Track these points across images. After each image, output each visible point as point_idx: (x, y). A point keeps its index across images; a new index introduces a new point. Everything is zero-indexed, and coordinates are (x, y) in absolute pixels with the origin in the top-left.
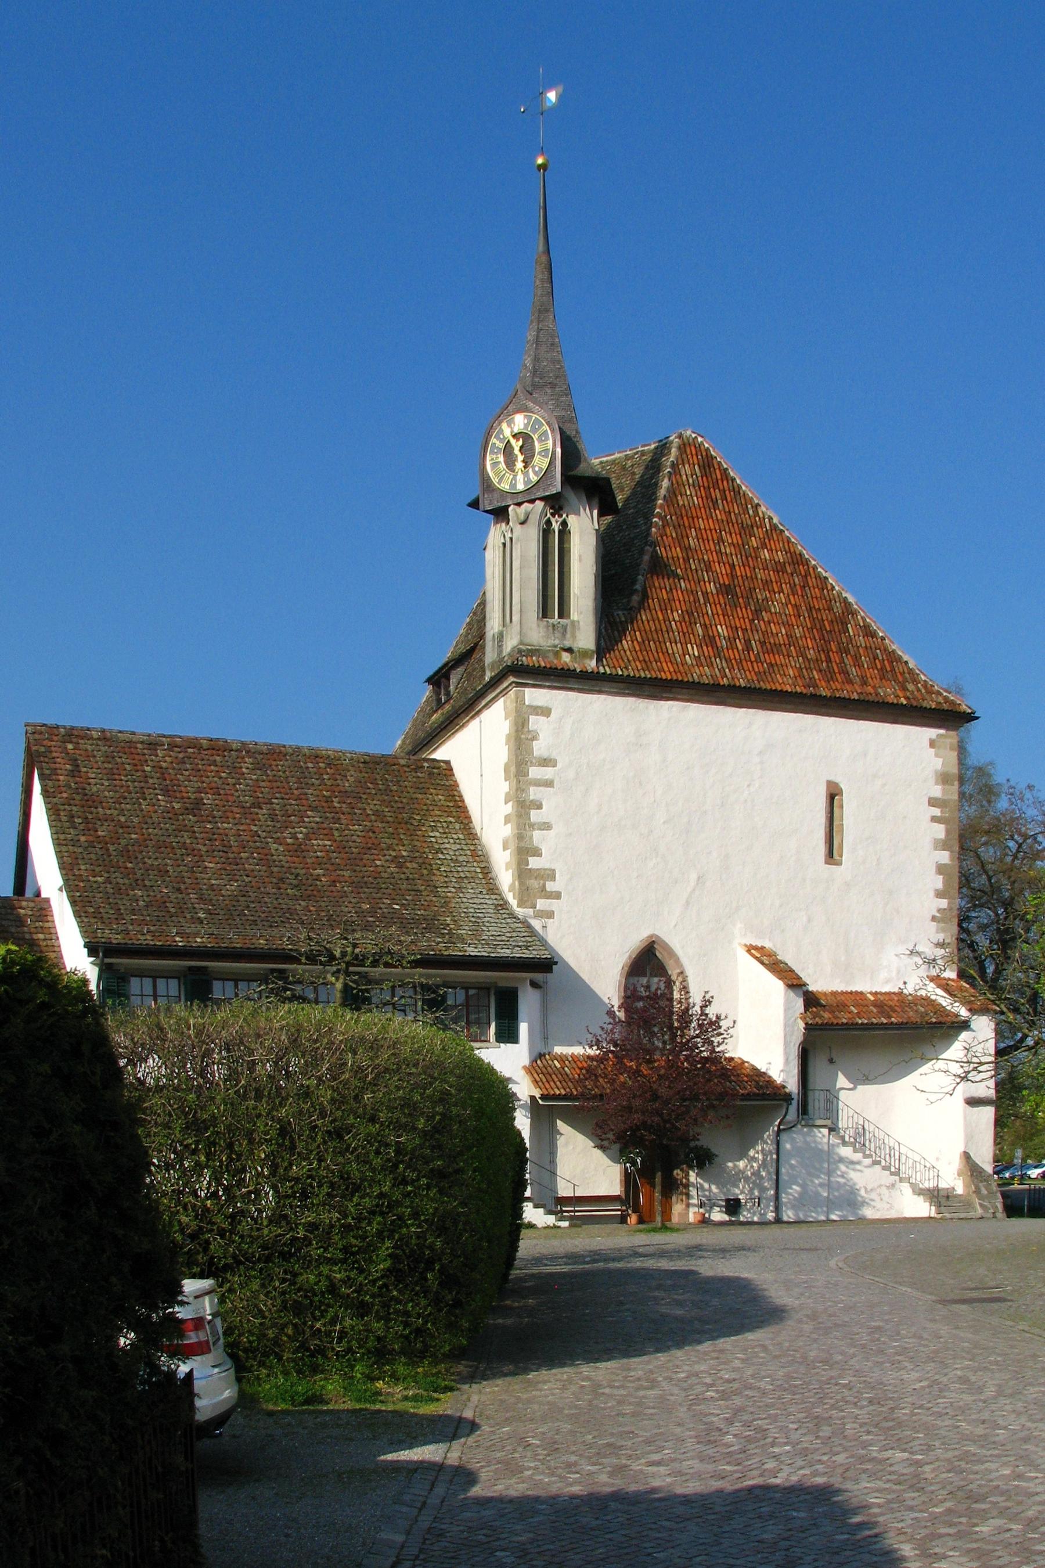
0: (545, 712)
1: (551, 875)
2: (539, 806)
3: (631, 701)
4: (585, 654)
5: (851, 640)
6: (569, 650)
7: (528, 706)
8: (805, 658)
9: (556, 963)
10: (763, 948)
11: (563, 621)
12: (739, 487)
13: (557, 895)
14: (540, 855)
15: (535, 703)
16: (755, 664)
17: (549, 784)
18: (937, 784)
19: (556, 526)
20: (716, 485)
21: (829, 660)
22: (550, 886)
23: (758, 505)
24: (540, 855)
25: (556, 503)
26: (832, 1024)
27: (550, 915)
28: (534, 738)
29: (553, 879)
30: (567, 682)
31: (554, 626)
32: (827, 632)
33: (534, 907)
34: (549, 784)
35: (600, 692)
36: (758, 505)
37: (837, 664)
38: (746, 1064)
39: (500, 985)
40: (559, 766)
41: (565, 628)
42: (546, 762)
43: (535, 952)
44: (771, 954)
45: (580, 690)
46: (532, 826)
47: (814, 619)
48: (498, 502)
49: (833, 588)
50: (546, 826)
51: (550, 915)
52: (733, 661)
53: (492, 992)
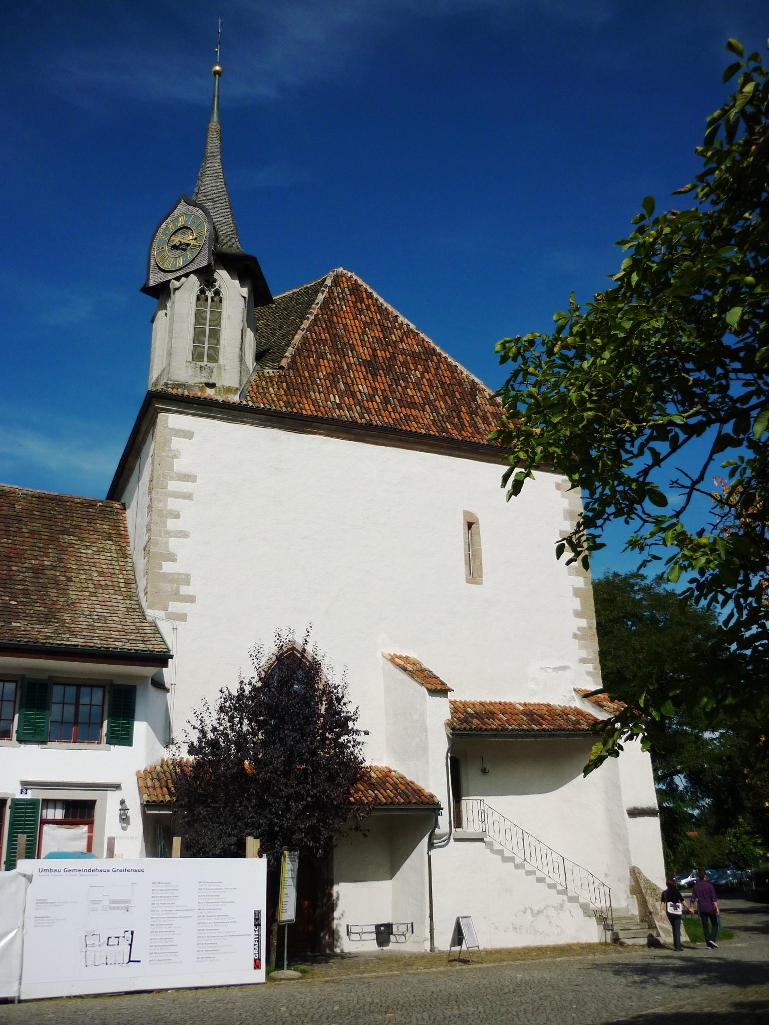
0: (189, 435)
1: (186, 579)
2: (177, 516)
4: (228, 390)
5: (480, 406)
6: (212, 386)
7: (170, 429)
8: (438, 414)
9: (171, 657)
10: (407, 658)
11: (211, 365)
12: (382, 304)
13: (191, 599)
14: (175, 560)
15: (177, 427)
16: (392, 413)
17: (188, 496)
18: (565, 519)
20: (362, 302)
21: (460, 417)
22: (184, 590)
23: (397, 316)
24: (175, 560)
25: (206, 276)
26: (481, 729)
27: (182, 617)
28: (175, 456)
29: (187, 583)
30: (210, 411)
31: (201, 367)
32: (458, 399)
33: (166, 609)
34: (188, 496)
35: (243, 422)
36: (397, 316)
37: (468, 421)
38: (393, 773)
39: (115, 683)
40: (199, 482)
41: (211, 371)
42: (189, 478)
43: (151, 646)
45: (222, 419)
46: (168, 534)
47: (446, 390)
48: (161, 279)
49: (462, 373)
50: (184, 535)
51: (182, 617)
52: (372, 410)
53: (107, 688)
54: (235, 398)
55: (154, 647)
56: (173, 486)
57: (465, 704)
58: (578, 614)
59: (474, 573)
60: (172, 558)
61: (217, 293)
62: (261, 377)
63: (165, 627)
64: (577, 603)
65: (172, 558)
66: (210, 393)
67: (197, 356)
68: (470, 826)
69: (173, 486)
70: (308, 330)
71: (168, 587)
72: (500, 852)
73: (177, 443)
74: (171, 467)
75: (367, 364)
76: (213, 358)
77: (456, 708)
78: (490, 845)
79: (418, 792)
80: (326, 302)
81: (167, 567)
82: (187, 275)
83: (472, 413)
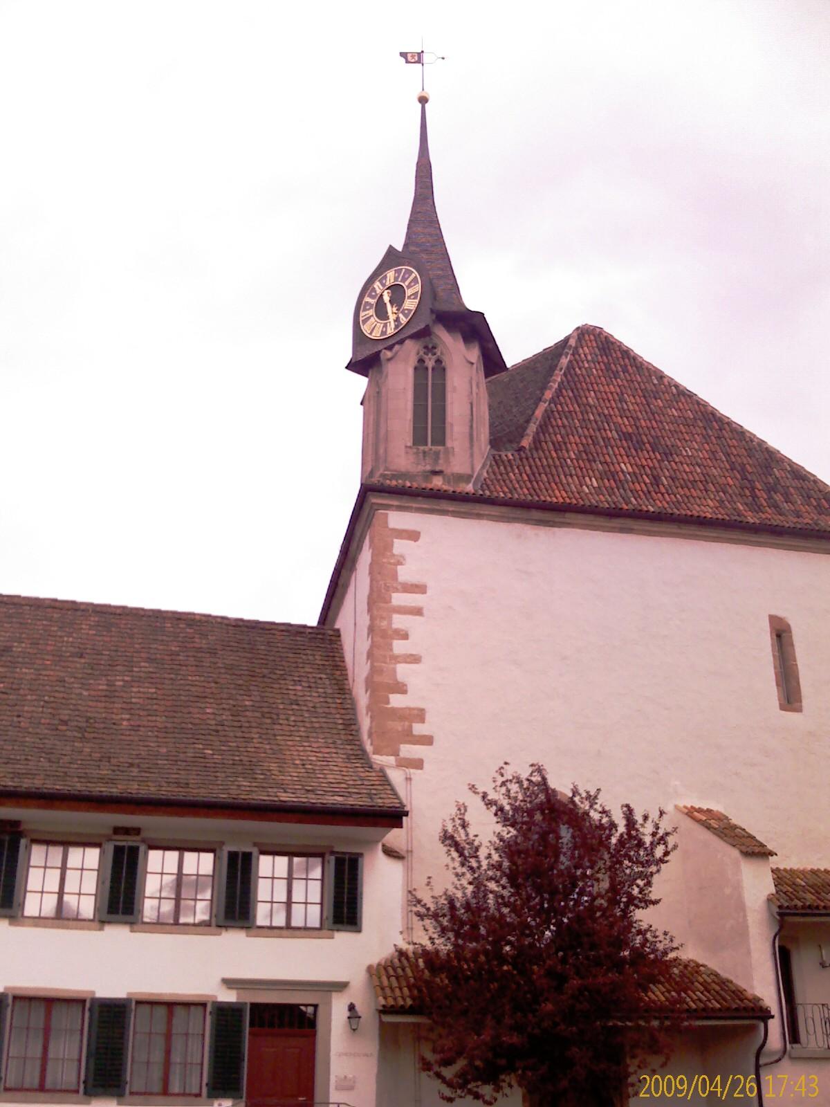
1: (420, 715)
2: (405, 636)
3: (517, 527)
9: (406, 814)
10: (709, 811)
13: (427, 740)
17: (418, 612)
19: (430, 364)
22: (418, 729)
26: (817, 907)
27: (418, 764)
28: (399, 563)
29: (422, 720)
31: (424, 452)
33: (396, 753)
34: (418, 612)
37: (765, 500)
38: (702, 968)
40: (429, 592)
41: (437, 454)
42: (420, 589)
43: (380, 801)
44: (721, 818)
46: (397, 659)
50: (415, 659)
51: (418, 764)
54: (469, 488)
55: (383, 801)
56: (398, 599)
57: (792, 872)
59: (790, 697)
60: (401, 689)
61: (439, 361)
62: (497, 461)
63: (396, 777)
65: (401, 689)
66: (437, 482)
67: (419, 437)
69: (398, 599)
70: (552, 401)
71: (398, 726)
73: (400, 546)
74: (395, 576)
76: (440, 439)
77: (781, 877)
79: (738, 994)
80: (570, 366)
81: (396, 701)
82: (401, 342)
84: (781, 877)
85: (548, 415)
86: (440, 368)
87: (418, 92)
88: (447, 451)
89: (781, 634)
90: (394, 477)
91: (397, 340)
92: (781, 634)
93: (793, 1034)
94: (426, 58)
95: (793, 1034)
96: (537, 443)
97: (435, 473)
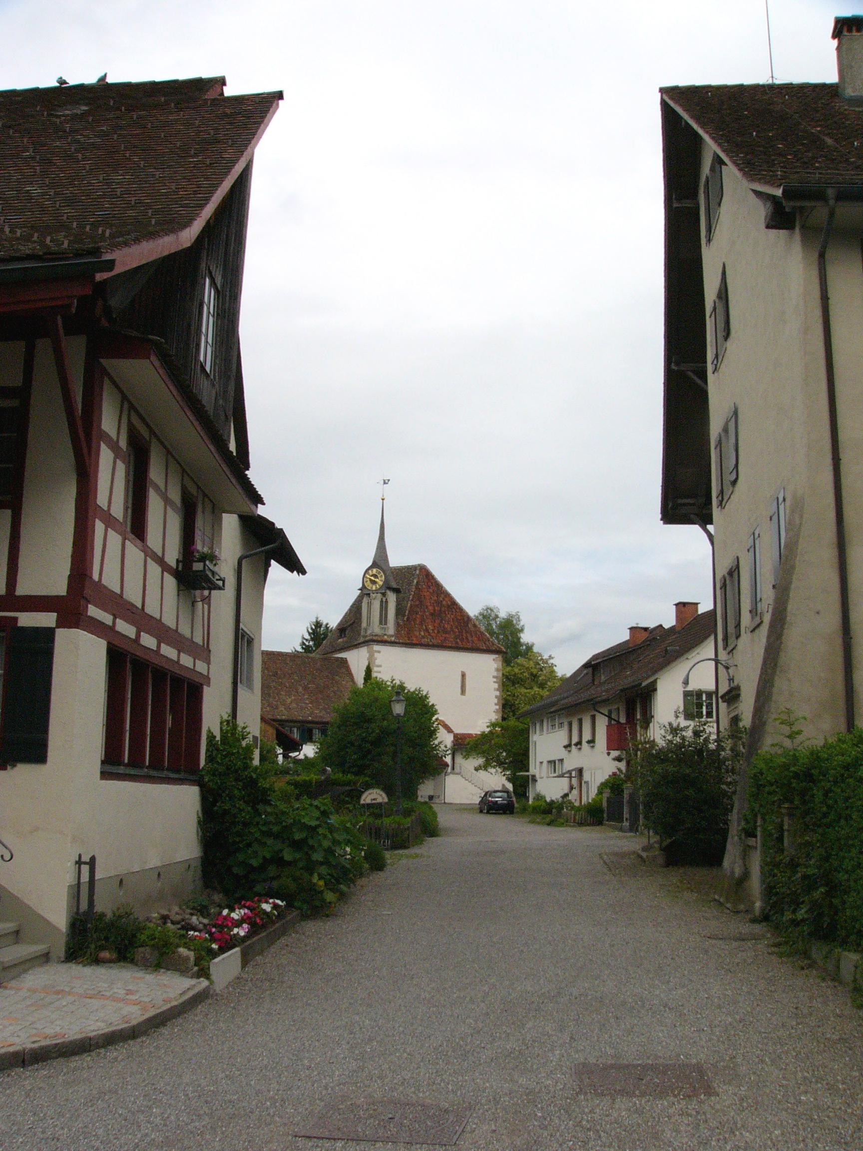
3: (404, 648)
4: (392, 636)
17: (380, 672)
19: (384, 600)
25: (384, 594)
41: (385, 629)
54: (393, 639)
57: (457, 734)
58: (496, 704)
59: (463, 692)
64: (496, 701)
66: (386, 637)
67: (381, 623)
68: (457, 769)
70: (412, 600)
72: (465, 778)
73: (376, 655)
75: (432, 614)
76: (386, 624)
77: (456, 736)
78: (462, 776)
83: (467, 632)
84: (456, 736)
85: (411, 606)
86: (387, 602)
87: (381, 497)
88: (388, 628)
89: (463, 675)
90: (376, 635)
91: (376, 591)
92: (463, 675)
93: (453, 768)
94: (382, 482)
95: (453, 768)
96: (408, 619)
97: (385, 635)
